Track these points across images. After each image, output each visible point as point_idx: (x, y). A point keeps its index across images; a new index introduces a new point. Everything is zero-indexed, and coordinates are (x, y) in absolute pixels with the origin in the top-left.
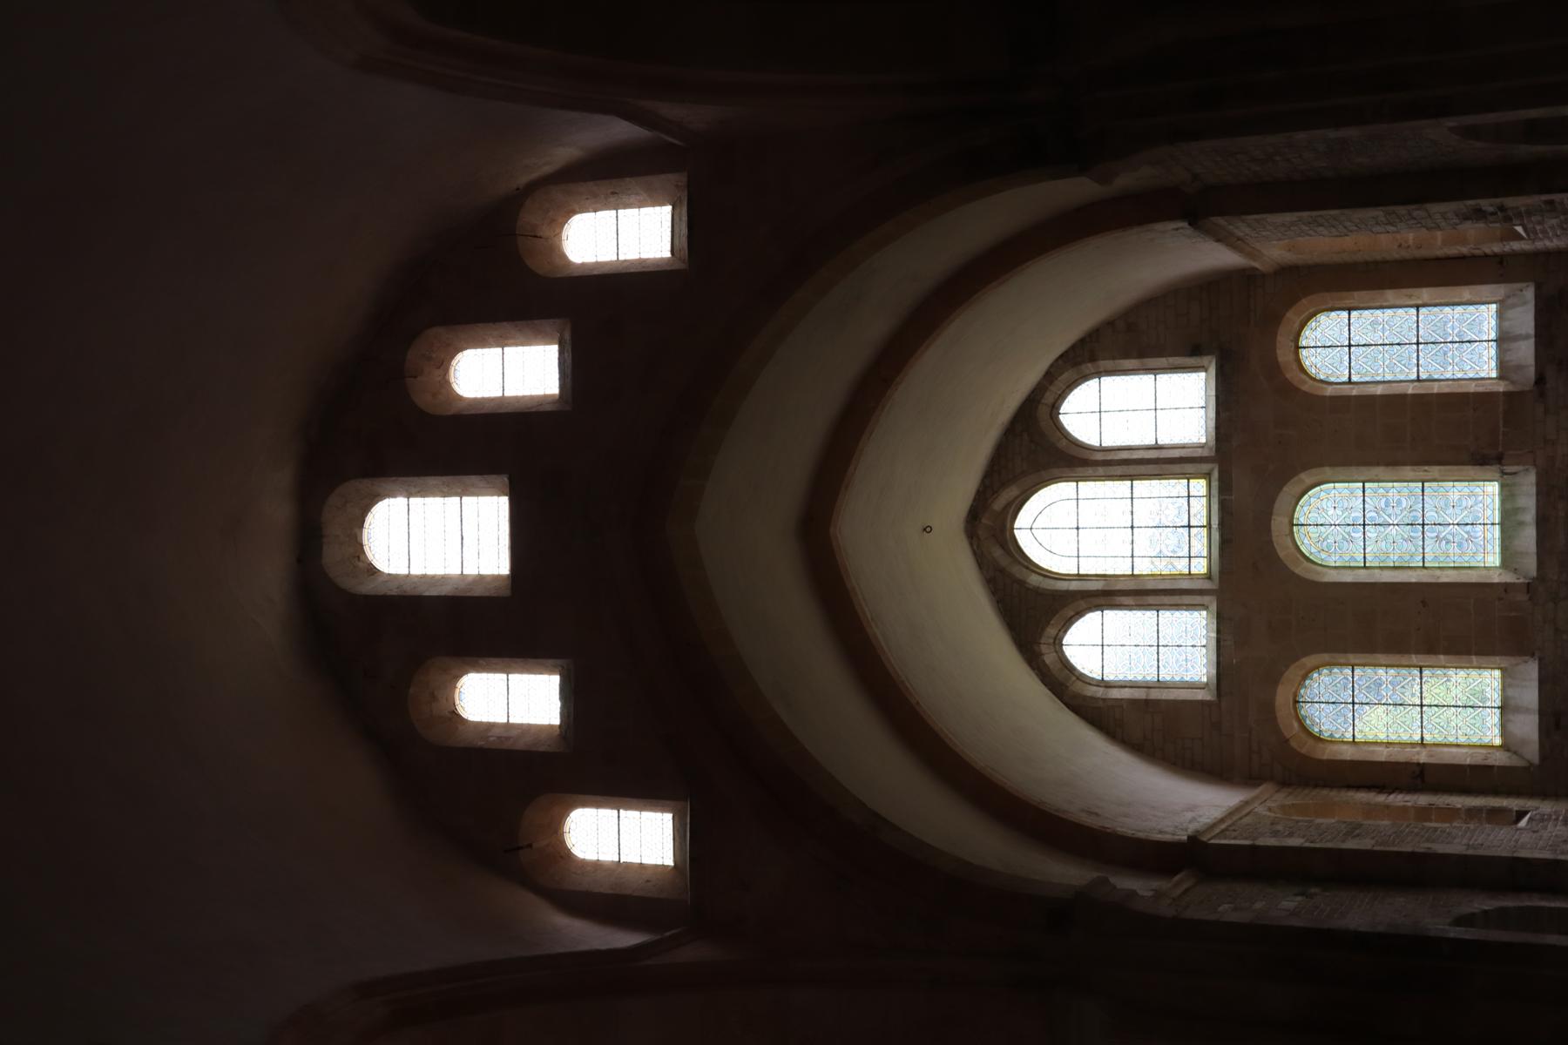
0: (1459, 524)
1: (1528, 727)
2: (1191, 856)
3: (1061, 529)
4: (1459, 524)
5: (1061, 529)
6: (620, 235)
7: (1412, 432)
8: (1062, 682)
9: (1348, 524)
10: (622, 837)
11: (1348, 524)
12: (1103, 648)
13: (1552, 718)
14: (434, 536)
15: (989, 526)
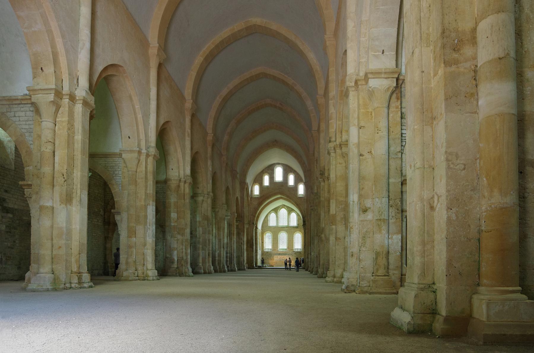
0: (283, 245)
1: (267, 250)
2: (257, 228)
3: (283, 212)
4: (283, 245)
5: (283, 212)
6: (301, 190)
7: (290, 242)
8: (270, 213)
9: (283, 236)
10: (256, 190)
11: (283, 236)
12: (273, 216)
13: (267, 252)
14: (279, 174)
15: (284, 206)
